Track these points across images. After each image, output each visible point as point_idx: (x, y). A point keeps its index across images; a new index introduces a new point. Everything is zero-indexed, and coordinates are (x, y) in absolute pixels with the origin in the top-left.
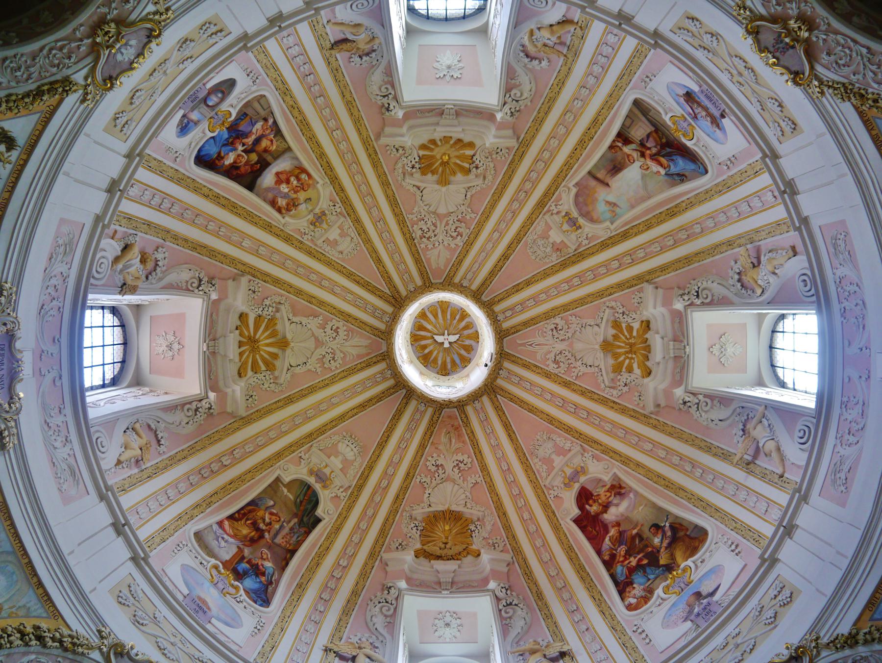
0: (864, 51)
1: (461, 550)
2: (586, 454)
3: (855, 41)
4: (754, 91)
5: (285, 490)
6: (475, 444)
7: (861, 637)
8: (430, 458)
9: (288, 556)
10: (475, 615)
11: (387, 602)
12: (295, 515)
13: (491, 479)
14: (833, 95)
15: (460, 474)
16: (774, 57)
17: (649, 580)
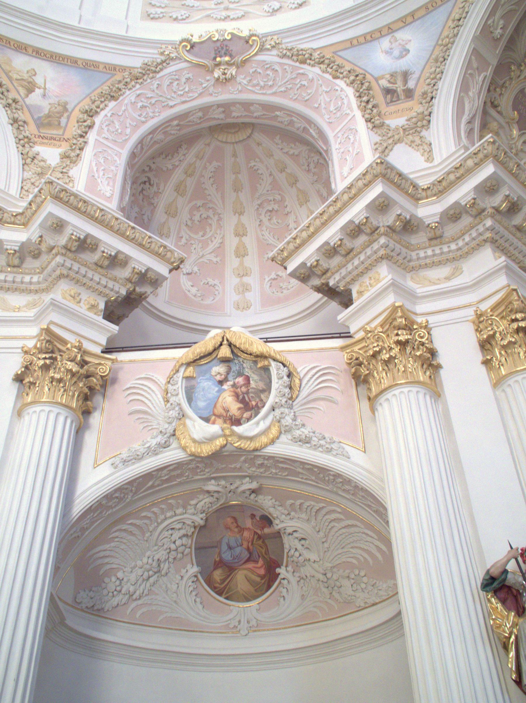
0: (171, 103)
3: (184, 102)
4: (205, 9)
14: (154, 60)
16: (218, 40)
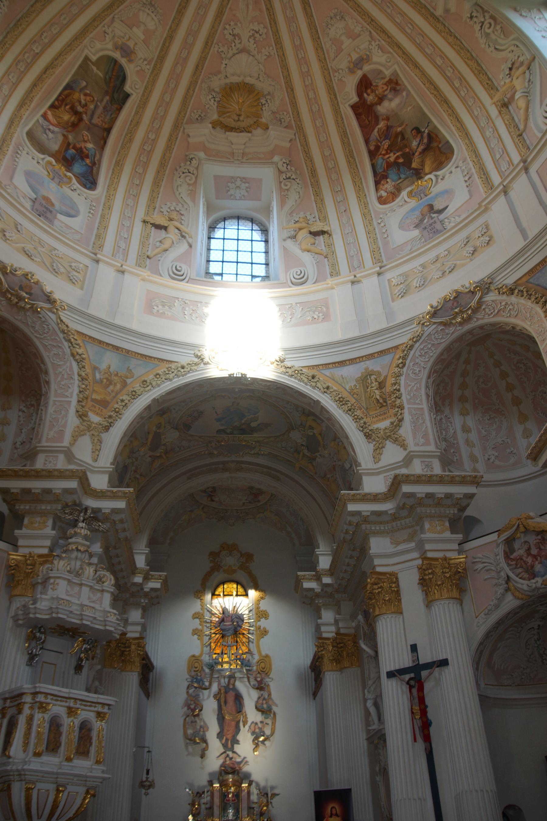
1: (252, 123)
2: (373, 43)
5: (95, 68)
6: (271, 14)
7: (516, 291)
8: (227, 27)
9: (105, 134)
10: (260, 180)
11: (189, 172)
12: (107, 93)
13: (283, 55)
15: (255, 45)
17: (400, 178)
